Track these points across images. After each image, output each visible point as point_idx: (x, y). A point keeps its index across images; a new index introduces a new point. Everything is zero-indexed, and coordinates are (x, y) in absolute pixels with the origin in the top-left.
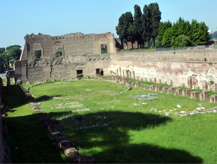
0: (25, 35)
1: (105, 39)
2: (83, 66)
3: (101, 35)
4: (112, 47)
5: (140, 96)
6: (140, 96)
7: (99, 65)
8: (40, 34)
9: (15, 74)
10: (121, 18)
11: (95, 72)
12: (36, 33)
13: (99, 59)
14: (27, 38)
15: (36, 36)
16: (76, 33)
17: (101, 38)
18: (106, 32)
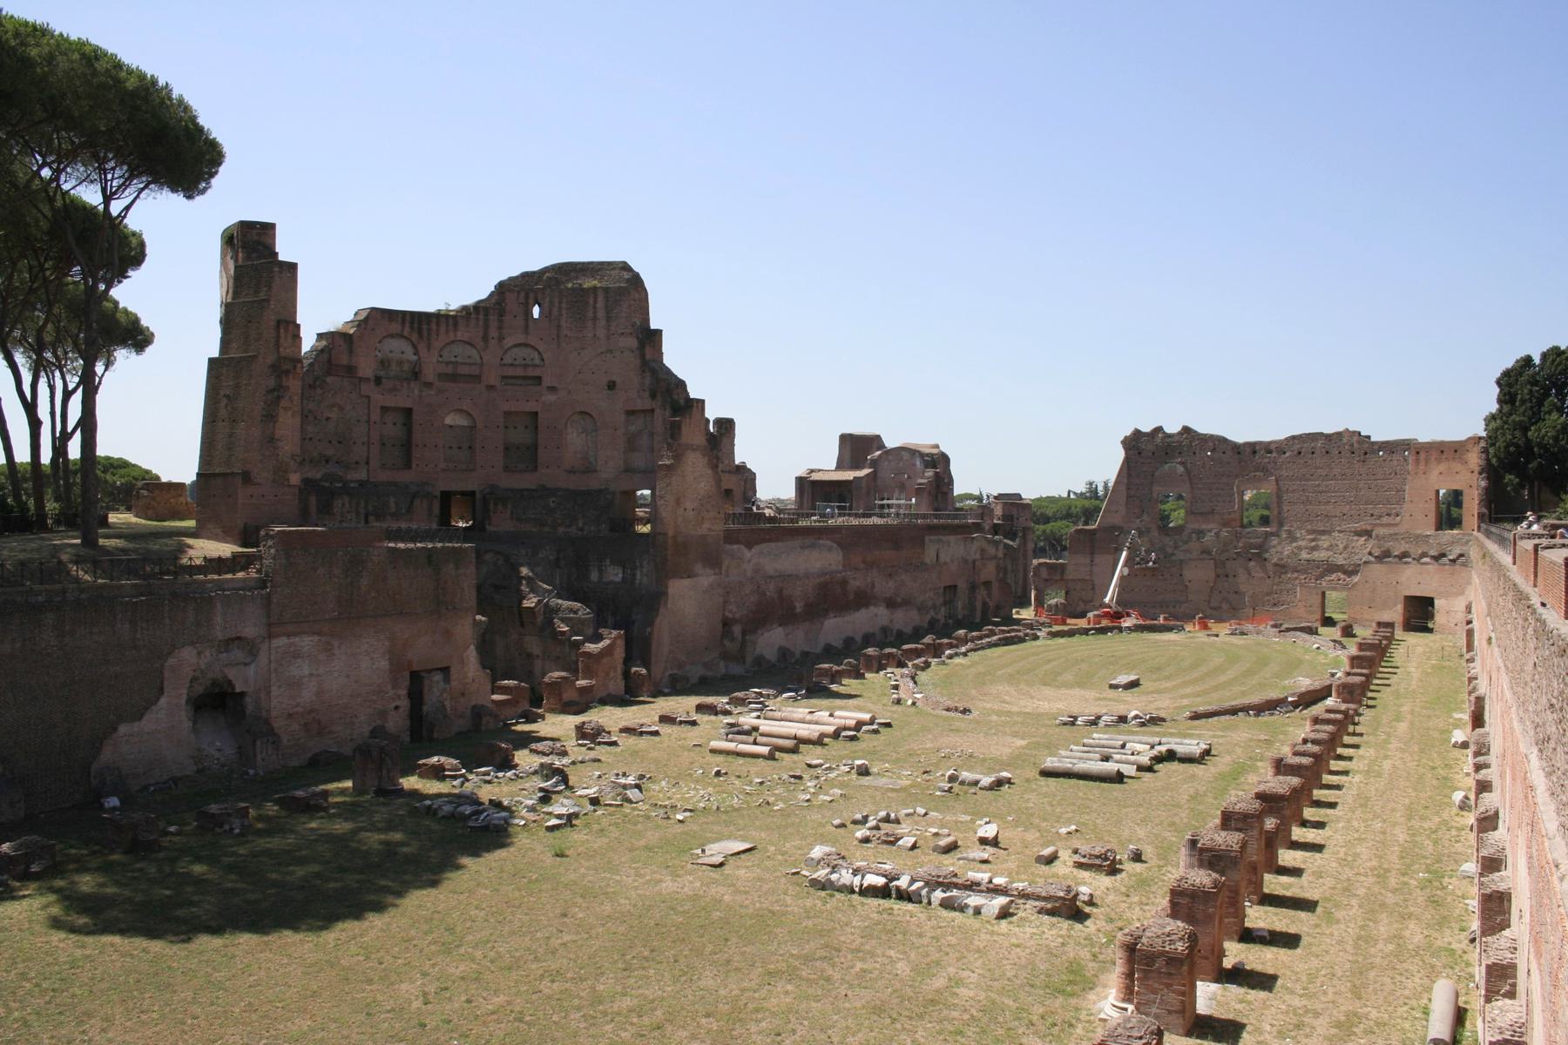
0: (1128, 433)
1: (1457, 466)
2: (1356, 579)
3: (1442, 443)
4: (1472, 506)
5: (1123, 746)
6: (1123, 746)
7: (1417, 580)
8: (1186, 430)
9: (1065, 577)
10: (1507, 374)
11: (1400, 608)
12: (1172, 428)
13: (1424, 555)
14: (1137, 445)
15: (1170, 436)
16: (1339, 434)
17: (1439, 461)
18: (1463, 437)
